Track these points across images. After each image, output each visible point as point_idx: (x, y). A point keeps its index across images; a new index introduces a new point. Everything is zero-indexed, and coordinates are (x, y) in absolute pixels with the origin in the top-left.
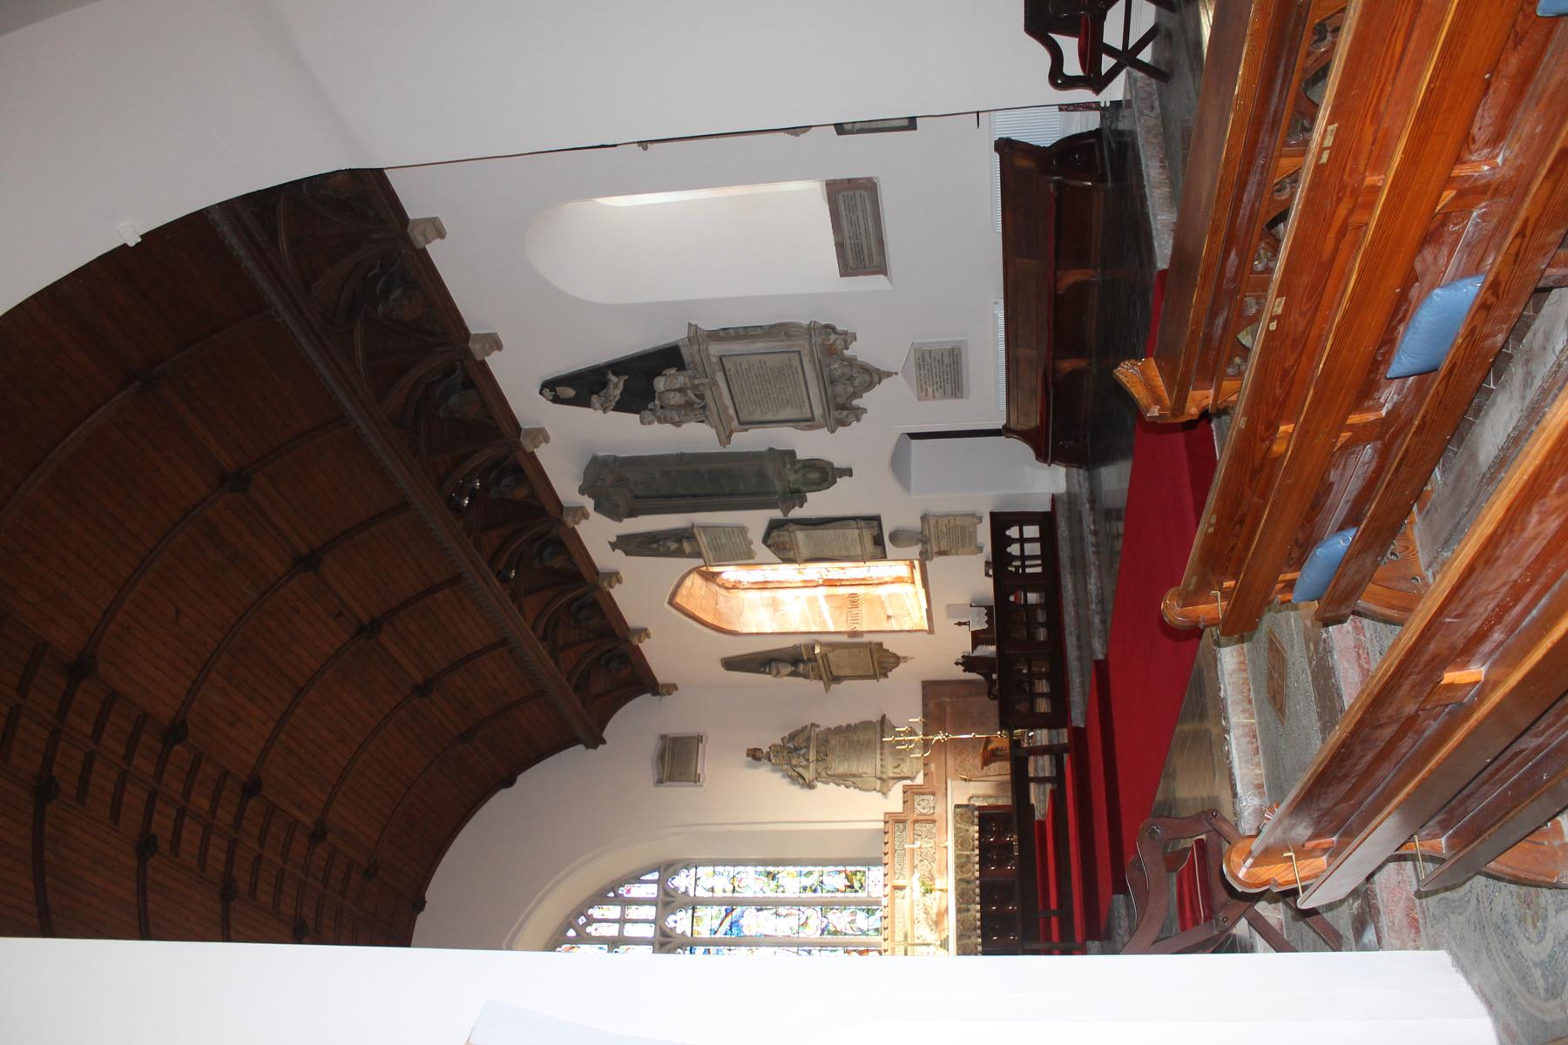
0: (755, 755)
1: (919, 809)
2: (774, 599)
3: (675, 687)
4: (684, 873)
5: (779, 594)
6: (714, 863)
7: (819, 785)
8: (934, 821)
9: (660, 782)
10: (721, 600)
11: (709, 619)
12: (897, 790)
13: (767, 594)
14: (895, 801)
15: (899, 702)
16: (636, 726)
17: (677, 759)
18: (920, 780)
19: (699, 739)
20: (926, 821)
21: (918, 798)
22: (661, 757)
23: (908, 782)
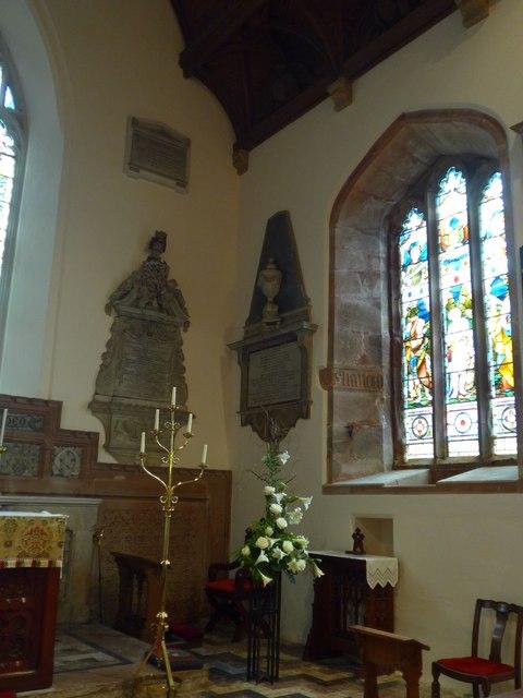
0: (158, 242)
1: (61, 453)
2: (377, 275)
3: (241, 167)
4: (11, 142)
5: (382, 285)
6: (18, 181)
7: (109, 320)
8: (40, 473)
9: (134, 122)
10: (380, 206)
11: (361, 182)
12: (92, 424)
13: (382, 267)
14: (77, 418)
15: (206, 438)
16: (196, 115)
17: (156, 151)
18: (104, 458)
19: (182, 183)
20: (42, 462)
21: (76, 452)
22: (164, 132)
23: (102, 441)
